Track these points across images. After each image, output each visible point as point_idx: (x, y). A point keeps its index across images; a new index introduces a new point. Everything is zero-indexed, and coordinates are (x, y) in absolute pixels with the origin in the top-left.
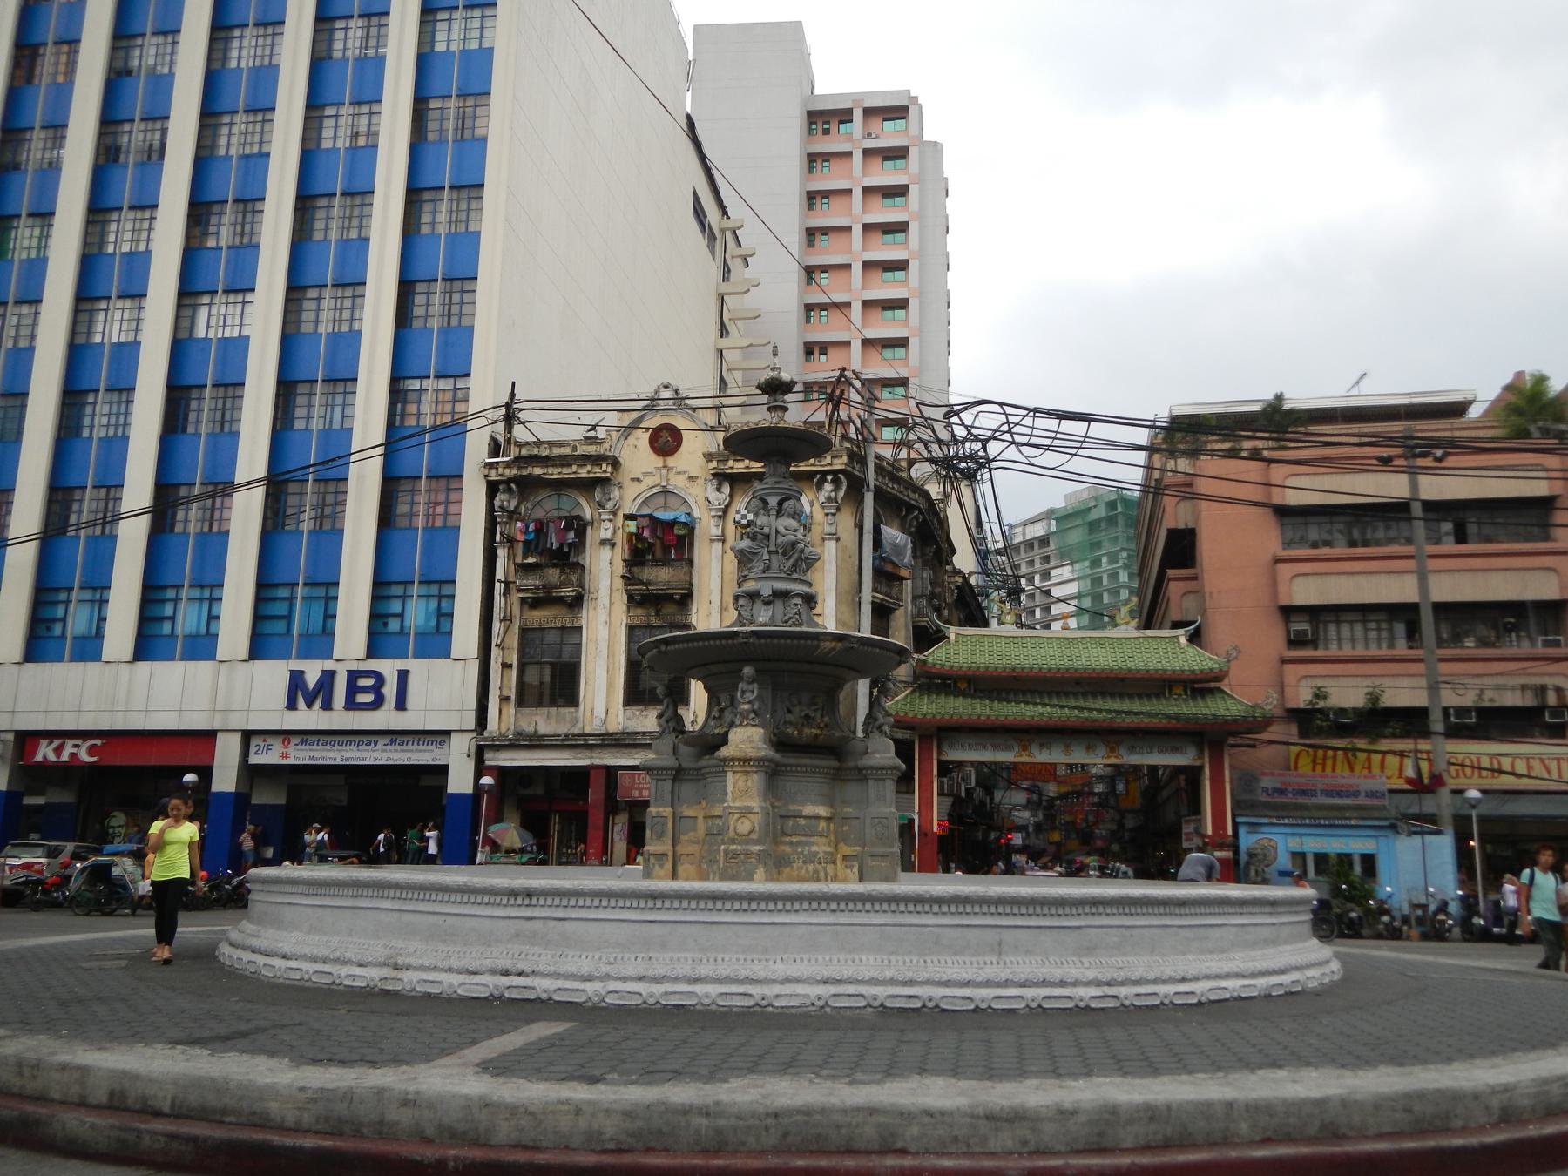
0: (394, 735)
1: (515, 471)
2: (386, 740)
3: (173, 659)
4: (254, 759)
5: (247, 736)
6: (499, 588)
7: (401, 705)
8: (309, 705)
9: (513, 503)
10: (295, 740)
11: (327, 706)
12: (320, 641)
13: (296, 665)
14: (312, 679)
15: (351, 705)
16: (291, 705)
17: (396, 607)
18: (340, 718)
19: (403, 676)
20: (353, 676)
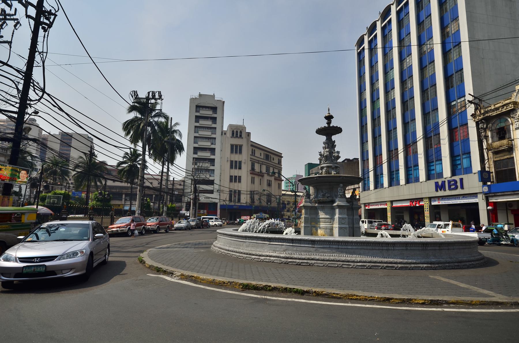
0: (464, 196)
1: (482, 116)
2: (462, 197)
3: (412, 182)
4: (433, 204)
5: (430, 199)
6: (485, 152)
7: (462, 187)
8: (441, 190)
9: (485, 126)
10: (441, 198)
11: (445, 190)
12: (440, 175)
13: (436, 181)
14: (440, 184)
15: (450, 189)
16: (437, 191)
17: (458, 162)
18: (448, 193)
19: (461, 180)
20: (449, 182)
